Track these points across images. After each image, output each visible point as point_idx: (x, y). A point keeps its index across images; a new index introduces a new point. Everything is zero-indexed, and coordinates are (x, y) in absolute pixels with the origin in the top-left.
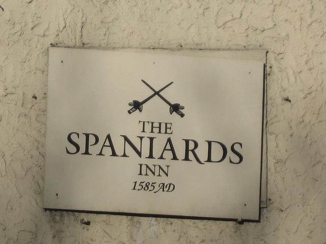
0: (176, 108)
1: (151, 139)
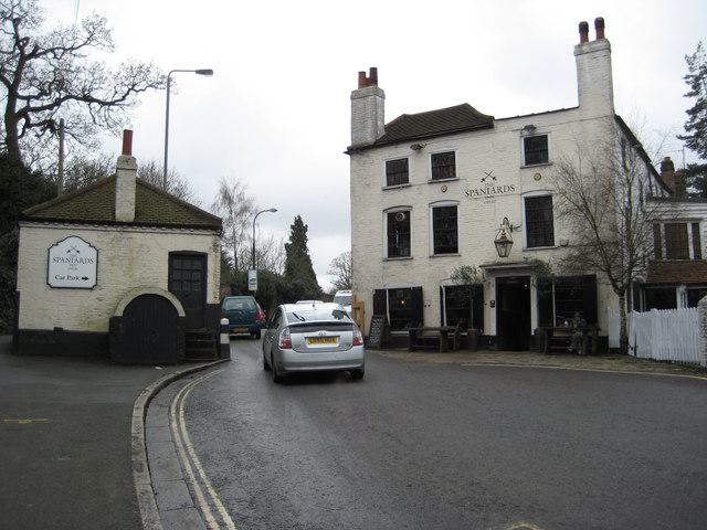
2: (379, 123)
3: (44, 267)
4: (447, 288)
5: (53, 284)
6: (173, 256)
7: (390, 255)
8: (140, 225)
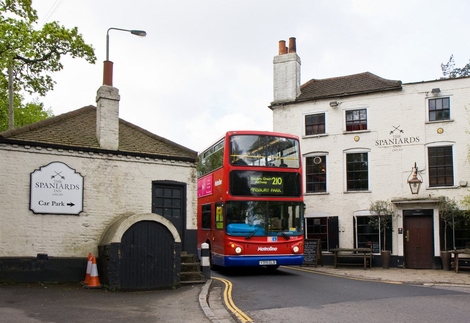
1: (396, 139)
2: (298, 84)
3: (26, 193)
5: (36, 210)
6: (157, 185)
8: (125, 154)
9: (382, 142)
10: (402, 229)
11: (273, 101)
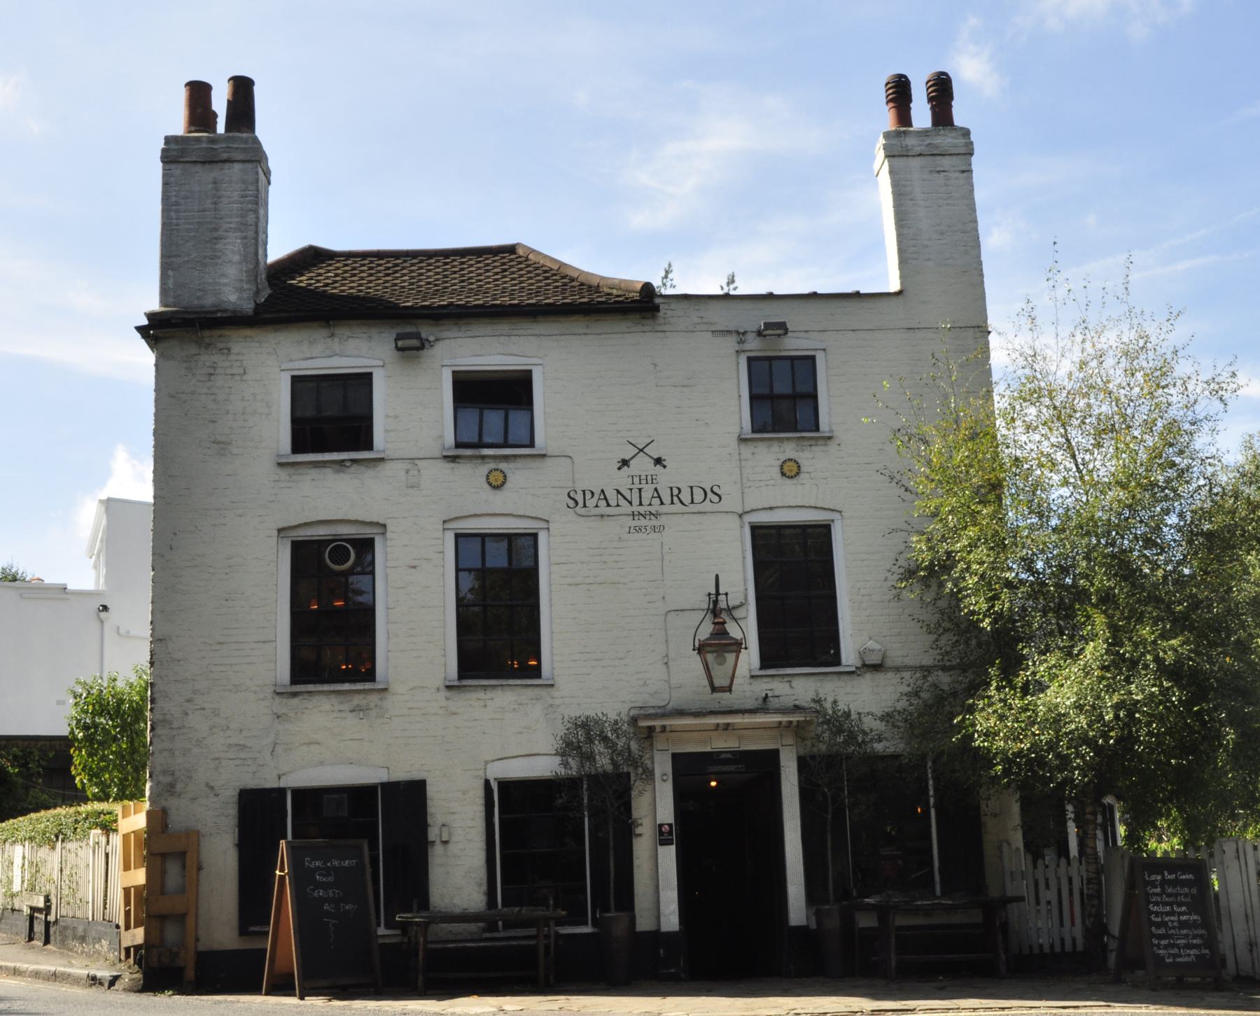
0: (658, 461)
1: (640, 490)
4: (505, 785)
7: (295, 679)
9: (588, 495)
10: (670, 825)
11: (155, 305)
